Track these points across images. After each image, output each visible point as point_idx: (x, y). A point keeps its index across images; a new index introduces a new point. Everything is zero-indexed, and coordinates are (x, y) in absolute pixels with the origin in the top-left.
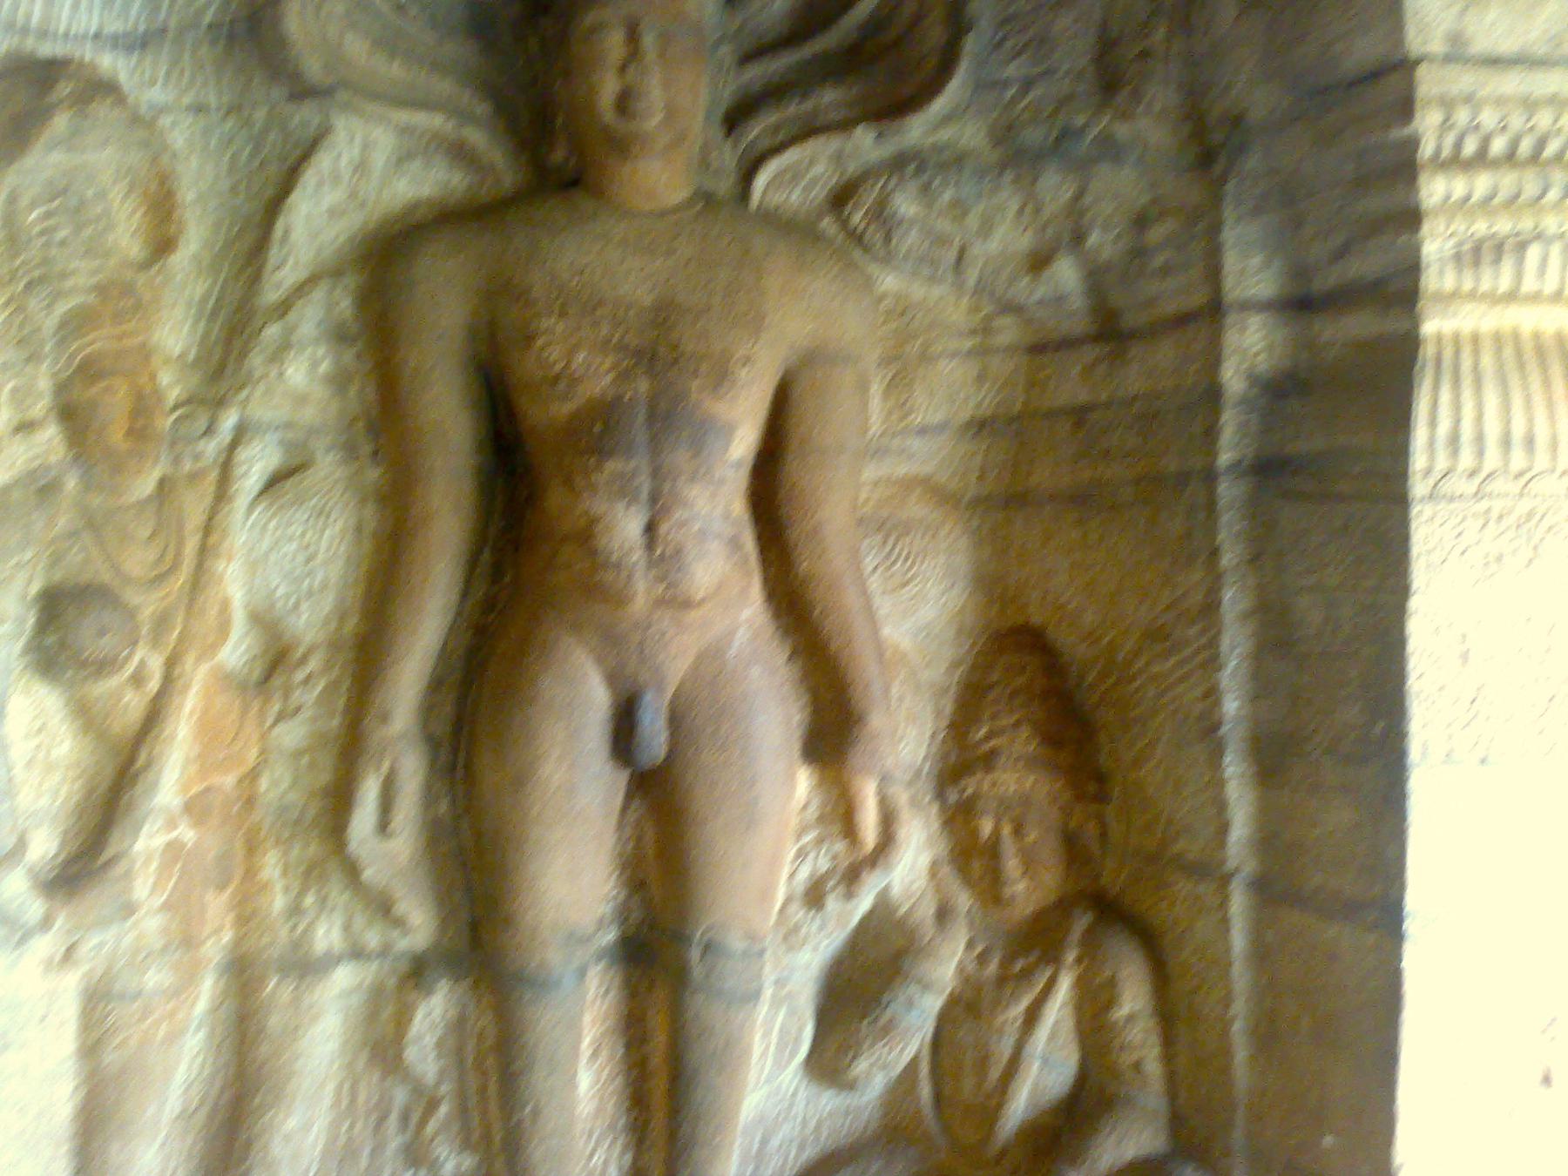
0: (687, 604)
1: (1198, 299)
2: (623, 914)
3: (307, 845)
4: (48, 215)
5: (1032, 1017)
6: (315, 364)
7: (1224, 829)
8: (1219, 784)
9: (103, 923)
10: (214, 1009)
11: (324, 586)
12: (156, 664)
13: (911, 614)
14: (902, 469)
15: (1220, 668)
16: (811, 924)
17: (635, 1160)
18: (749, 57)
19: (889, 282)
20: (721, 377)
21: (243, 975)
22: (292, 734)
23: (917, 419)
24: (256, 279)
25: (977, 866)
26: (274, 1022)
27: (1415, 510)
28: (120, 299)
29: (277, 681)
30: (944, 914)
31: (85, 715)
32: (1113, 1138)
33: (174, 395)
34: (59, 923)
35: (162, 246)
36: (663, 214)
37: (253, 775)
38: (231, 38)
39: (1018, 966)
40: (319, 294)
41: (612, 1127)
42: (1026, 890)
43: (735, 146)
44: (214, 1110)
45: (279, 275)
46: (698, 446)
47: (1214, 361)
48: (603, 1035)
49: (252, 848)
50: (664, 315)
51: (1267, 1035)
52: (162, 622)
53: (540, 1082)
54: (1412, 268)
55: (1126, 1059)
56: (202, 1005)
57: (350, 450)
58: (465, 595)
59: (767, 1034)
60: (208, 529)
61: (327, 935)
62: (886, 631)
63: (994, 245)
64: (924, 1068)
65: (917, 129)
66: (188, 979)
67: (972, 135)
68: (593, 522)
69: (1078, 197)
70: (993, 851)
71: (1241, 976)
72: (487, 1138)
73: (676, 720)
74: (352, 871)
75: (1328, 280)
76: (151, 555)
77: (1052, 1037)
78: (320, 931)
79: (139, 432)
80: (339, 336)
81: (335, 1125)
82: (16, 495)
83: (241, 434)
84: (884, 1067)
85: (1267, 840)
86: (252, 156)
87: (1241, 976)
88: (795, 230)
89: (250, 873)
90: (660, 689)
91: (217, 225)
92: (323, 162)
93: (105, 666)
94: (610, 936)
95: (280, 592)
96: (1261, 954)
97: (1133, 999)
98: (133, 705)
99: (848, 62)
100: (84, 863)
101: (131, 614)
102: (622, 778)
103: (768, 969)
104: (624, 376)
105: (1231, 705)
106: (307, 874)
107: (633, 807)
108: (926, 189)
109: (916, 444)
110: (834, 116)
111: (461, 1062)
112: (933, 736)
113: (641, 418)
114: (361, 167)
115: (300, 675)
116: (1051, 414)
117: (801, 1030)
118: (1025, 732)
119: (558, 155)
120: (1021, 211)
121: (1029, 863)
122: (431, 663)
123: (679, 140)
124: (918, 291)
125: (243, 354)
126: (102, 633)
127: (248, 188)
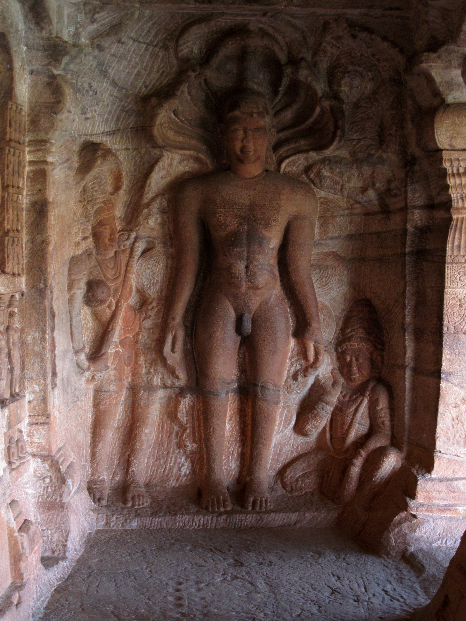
0: (257, 288)
1: (403, 205)
2: (239, 380)
3: (152, 354)
4: (94, 184)
5: (356, 410)
6: (156, 220)
7: (405, 353)
8: (405, 340)
9: (101, 370)
10: (126, 399)
11: (157, 281)
12: (114, 302)
13: (328, 295)
14: (326, 250)
15: (405, 309)
16: (294, 385)
17: (242, 451)
18: (279, 131)
19: (323, 194)
20: (268, 225)
21: (134, 390)
22: (148, 324)
23: (330, 235)
24: (141, 196)
25: (345, 370)
26: (142, 403)
27: (447, 265)
28: (109, 204)
29: (144, 309)
30: (335, 383)
31: (96, 315)
32: (374, 442)
33: (119, 228)
34: (92, 368)
35: (117, 188)
36: (253, 178)
37: (138, 334)
38: (137, 130)
39: (354, 397)
40: (158, 201)
41: (236, 440)
42: (358, 377)
43: (276, 155)
44: (126, 427)
45: (148, 195)
46: (260, 245)
47: (405, 222)
48: (232, 414)
49: (137, 355)
50: (252, 207)
51: (414, 410)
52: (116, 290)
53: (215, 421)
54: (450, 200)
55: (380, 421)
56: (123, 399)
57: (165, 244)
58: (195, 285)
59: (281, 417)
60: (127, 266)
61: (157, 380)
62: (319, 299)
63: (352, 185)
64: (328, 429)
65: (328, 152)
66: (121, 390)
67: (344, 153)
68: (231, 265)
69: (373, 172)
70: (349, 365)
71: (408, 396)
72: (200, 439)
73: (254, 321)
74: (164, 361)
75: (437, 201)
76: (113, 272)
77: (361, 417)
78: (155, 379)
79: (111, 240)
80: (163, 212)
81: (157, 436)
82: (84, 256)
83: (136, 239)
84: (315, 427)
85: (417, 357)
86: (140, 161)
87: (408, 396)
88: (292, 180)
89: (136, 362)
90: (249, 313)
91: (130, 181)
92: (160, 164)
93: (102, 302)
94: (235, 386)
95: (145, 284)
96: (414, 388)
97: (383, 404)
98: (108, 313)
99: (309, 133)
100: (96, 354)
101: (109, 288)
102: (239, 338)
103: (281, 398)
104: (241, 224)
105: (408, 320)
106: (151, 364)
107: (242, 348)
108: (331, 168)
109: (330, 242)
110: (304, 148)
111: (193, 418)
112: (336, 331)
113: (245, 236)
114: (170, 165)
115: (150, 307)
116: (371, 234)
117: (292, 416)
118: (361, 330)
119: (225, 161)
120: (358, 176)
121: (360, 368)
122: (186, 305)
123: (258, 158)
124: (331, 196)
125: (138, 217)
126: (103, 293)
127: (139, 170)
